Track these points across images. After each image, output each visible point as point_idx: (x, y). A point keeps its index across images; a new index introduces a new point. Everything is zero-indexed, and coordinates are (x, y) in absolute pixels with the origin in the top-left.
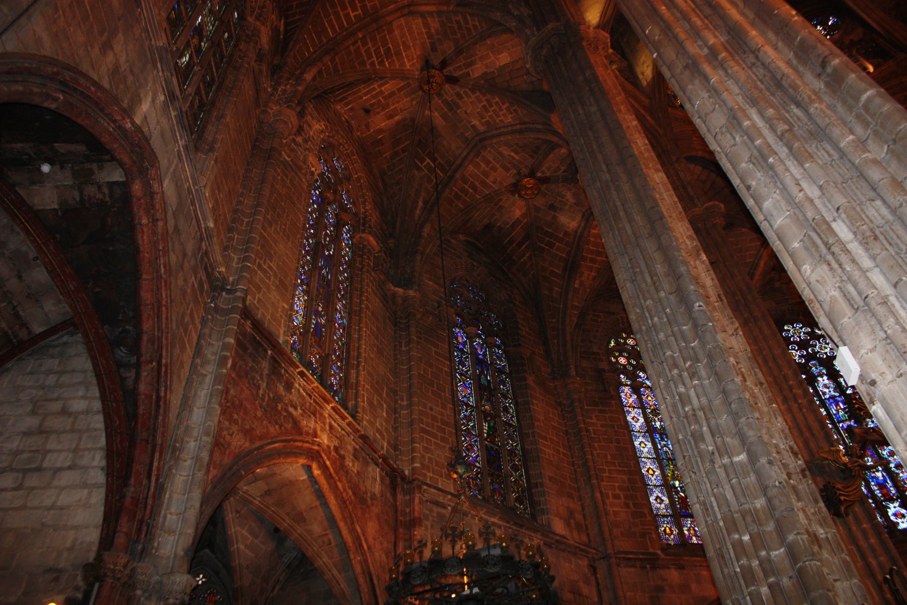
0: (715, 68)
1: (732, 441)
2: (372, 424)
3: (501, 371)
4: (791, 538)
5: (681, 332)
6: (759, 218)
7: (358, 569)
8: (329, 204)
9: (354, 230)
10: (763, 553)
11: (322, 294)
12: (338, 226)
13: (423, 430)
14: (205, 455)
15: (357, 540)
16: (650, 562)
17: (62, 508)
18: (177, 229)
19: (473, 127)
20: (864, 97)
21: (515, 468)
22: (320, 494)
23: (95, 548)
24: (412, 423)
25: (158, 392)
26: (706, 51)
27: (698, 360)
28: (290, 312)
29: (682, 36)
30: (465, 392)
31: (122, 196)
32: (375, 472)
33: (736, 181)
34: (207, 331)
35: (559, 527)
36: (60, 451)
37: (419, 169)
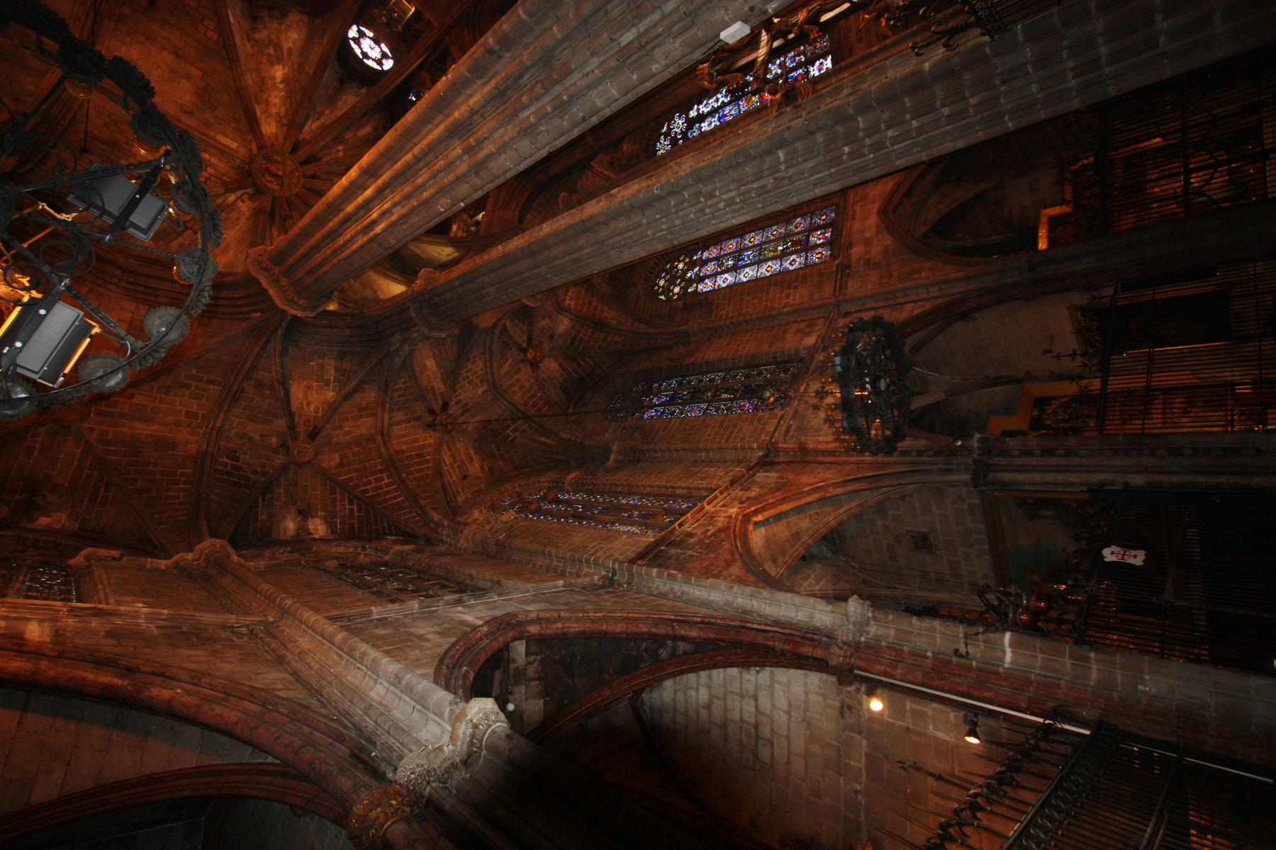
0: (481, 149)
1: (768, 161)
2: (721, 478)
3: (680, 384)
4: (851, 110)
5: (676, 205)
6: (608, 112)
7: (840, 490)
9: (562, 490)
10: (861, 134)
11: (615, 512)
12: (558, 502)
13: (727, 441)
14: (748, 590)
15: (816, 490)
16: (845, 270)
17: (790, 706)
18: (567, 604)
19: (484, 393)
20: (523, 17)
21: (760, 374)
22: (778, 517)
23: (824, 676)
24: (720, 449)
25: (696, 623)
26: (465, 157)
27: (699, 193)
28: (631, 537)
29: (452, 177)
30: (694, 412)
31: (539, 643)
32: (760, 476)
33: (576, 132)
34: (646, 590)
35: (810, 341)
36: (741, 709)
37: (514, 439)
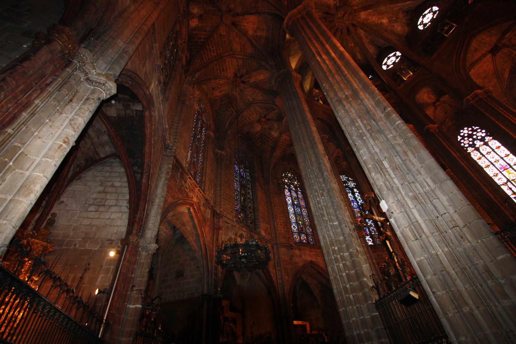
0: (347, 103)
1: (334, 218)
2: (209, 195)
3: (248, 180)
5: (319, 181)
6: (357, 155)
7: (202, 243)
8: (199, 120)
9: (206, 130)
11: (196, 151)
12: (201, 128)
13: (224, 198)
14: (162, 204)
15: (202, 233)
18: (158, 128)
21: (251, 213)
22: (191, 217)
24: (221, 196)
25: (148, 182)
26: (344, 96)
27: (323, 190)
28: (186, 157)
29: (337, 90)
30: (236, 186)
31: (141, 115)
32: (209, 211)
33: (351, 142)
34: (163, 162)
35: (263, 233)
37: (229, 111)
